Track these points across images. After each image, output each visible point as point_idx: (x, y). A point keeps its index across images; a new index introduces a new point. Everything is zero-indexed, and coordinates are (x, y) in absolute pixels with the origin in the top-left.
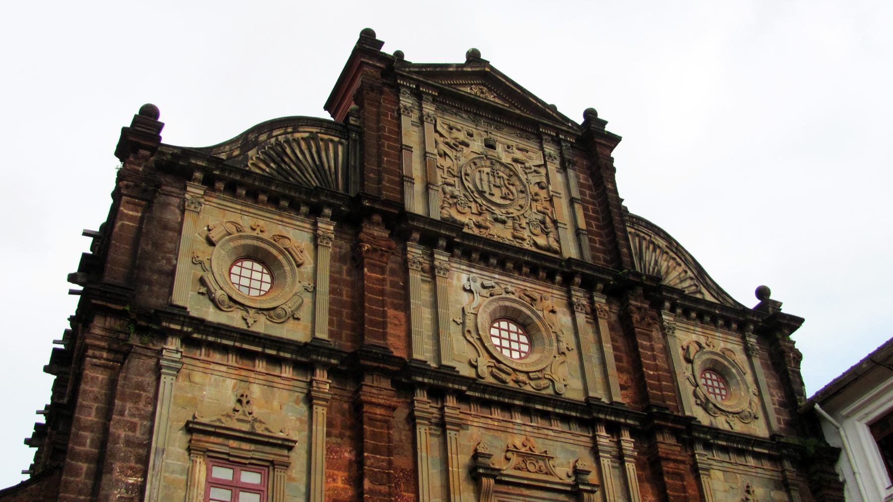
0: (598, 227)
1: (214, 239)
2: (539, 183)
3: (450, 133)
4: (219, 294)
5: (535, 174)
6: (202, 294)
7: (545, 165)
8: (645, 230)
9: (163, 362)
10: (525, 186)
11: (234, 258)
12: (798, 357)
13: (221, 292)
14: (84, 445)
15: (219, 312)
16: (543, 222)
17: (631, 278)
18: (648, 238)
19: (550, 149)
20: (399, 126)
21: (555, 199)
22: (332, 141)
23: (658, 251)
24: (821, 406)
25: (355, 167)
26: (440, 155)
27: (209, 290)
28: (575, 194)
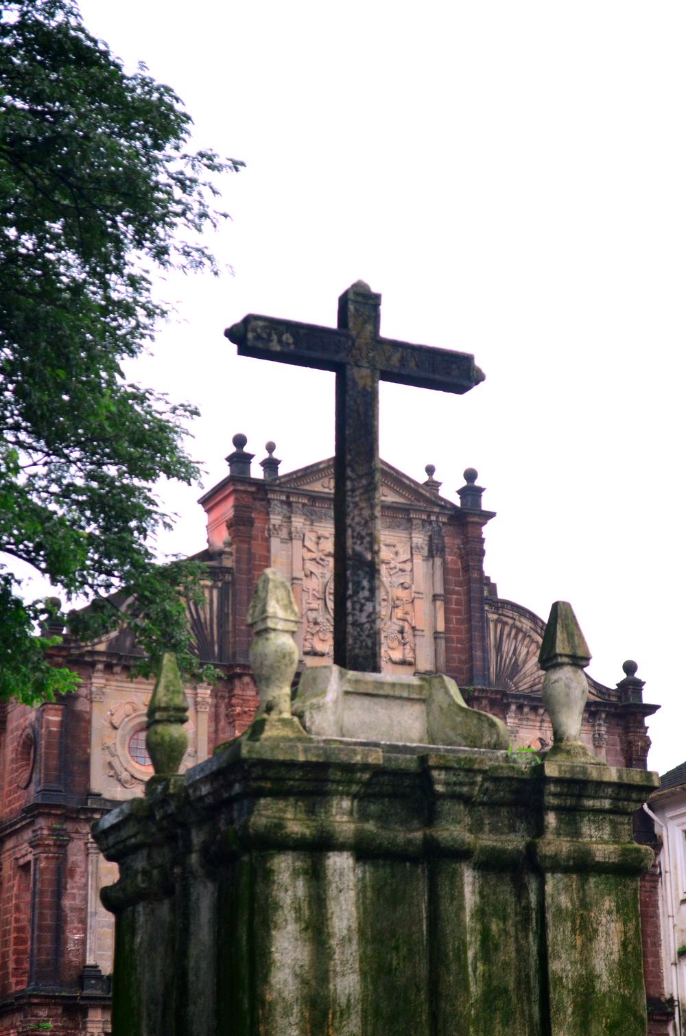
0: (458, 621)
1: (116, 725)
2: (402, 584)
3: (318, 544)
4: (125, 776)
5: (401, 573)
6: (111, 776)
7: (411, 560)
8: (509, 613)
9: (89, 845)
10: (388, 592)
11: (132, 733)
12: (647, 744)
13: (126, 773)
14: (46, 920)
15: (124, 789)
16: (402, 632)
17: (476, 694)
18: (510, 621)
19: (420, 538)
20: (269, 551)
21: (416, 601)
22: (207, 587)
23: (520, 636)
24: (649, 807)
25: (228, 614)
26: (306, 576)
27: (116, 773)
28: (439, 590)
